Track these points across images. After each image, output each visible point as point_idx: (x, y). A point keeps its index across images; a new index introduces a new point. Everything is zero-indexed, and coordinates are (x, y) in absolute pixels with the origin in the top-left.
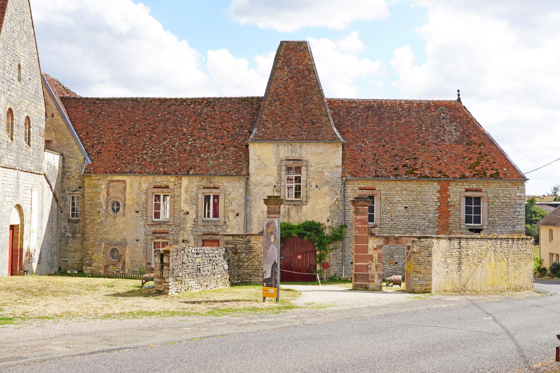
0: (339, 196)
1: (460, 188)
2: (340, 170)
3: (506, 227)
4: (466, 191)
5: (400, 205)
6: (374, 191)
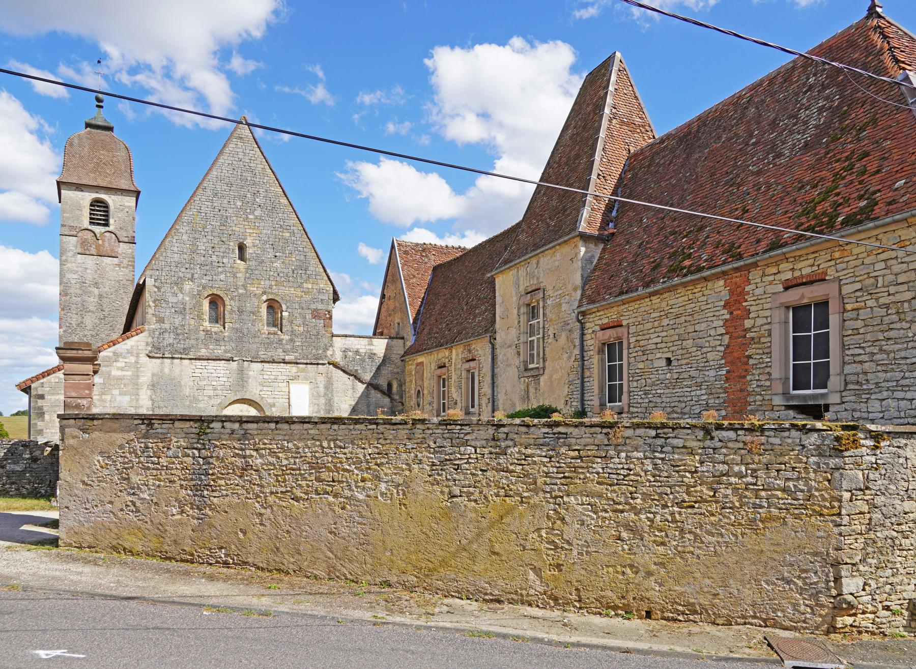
0: (577, 351)
1: (771, 283)
2: (579, 293)
3: (900, 395)
4: (786, 288)
5: (658, 355)
6: (619, 329)
